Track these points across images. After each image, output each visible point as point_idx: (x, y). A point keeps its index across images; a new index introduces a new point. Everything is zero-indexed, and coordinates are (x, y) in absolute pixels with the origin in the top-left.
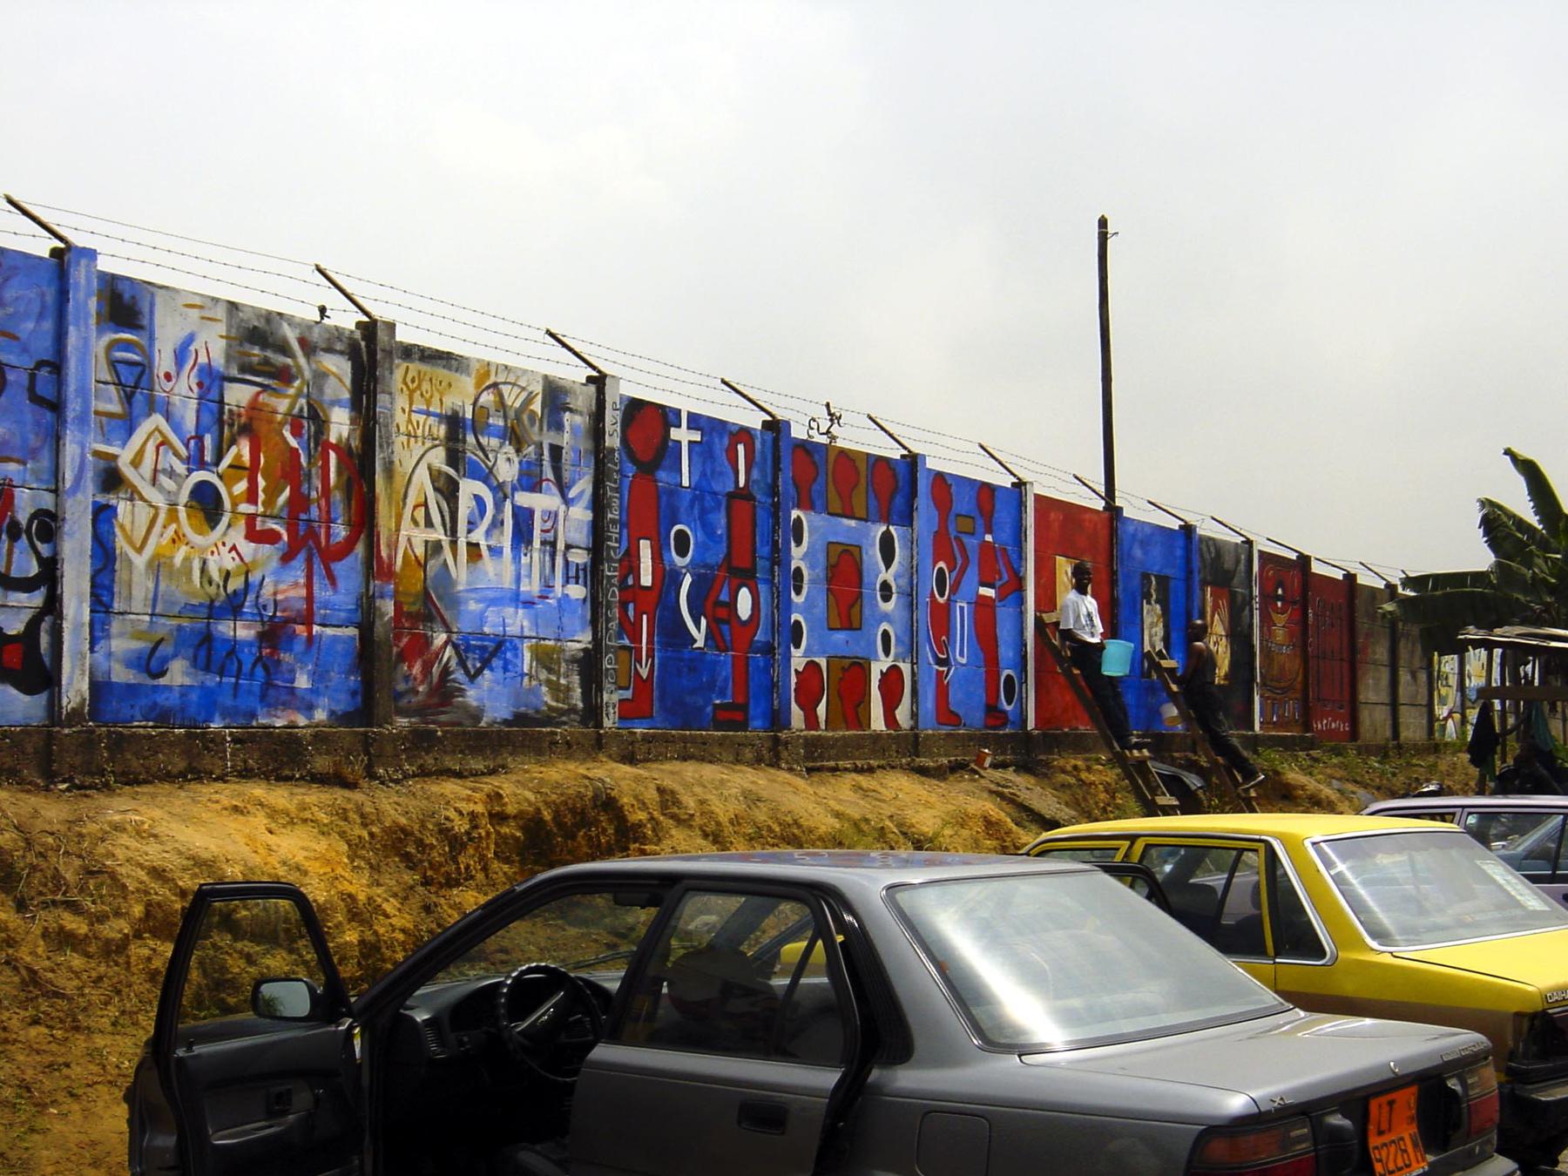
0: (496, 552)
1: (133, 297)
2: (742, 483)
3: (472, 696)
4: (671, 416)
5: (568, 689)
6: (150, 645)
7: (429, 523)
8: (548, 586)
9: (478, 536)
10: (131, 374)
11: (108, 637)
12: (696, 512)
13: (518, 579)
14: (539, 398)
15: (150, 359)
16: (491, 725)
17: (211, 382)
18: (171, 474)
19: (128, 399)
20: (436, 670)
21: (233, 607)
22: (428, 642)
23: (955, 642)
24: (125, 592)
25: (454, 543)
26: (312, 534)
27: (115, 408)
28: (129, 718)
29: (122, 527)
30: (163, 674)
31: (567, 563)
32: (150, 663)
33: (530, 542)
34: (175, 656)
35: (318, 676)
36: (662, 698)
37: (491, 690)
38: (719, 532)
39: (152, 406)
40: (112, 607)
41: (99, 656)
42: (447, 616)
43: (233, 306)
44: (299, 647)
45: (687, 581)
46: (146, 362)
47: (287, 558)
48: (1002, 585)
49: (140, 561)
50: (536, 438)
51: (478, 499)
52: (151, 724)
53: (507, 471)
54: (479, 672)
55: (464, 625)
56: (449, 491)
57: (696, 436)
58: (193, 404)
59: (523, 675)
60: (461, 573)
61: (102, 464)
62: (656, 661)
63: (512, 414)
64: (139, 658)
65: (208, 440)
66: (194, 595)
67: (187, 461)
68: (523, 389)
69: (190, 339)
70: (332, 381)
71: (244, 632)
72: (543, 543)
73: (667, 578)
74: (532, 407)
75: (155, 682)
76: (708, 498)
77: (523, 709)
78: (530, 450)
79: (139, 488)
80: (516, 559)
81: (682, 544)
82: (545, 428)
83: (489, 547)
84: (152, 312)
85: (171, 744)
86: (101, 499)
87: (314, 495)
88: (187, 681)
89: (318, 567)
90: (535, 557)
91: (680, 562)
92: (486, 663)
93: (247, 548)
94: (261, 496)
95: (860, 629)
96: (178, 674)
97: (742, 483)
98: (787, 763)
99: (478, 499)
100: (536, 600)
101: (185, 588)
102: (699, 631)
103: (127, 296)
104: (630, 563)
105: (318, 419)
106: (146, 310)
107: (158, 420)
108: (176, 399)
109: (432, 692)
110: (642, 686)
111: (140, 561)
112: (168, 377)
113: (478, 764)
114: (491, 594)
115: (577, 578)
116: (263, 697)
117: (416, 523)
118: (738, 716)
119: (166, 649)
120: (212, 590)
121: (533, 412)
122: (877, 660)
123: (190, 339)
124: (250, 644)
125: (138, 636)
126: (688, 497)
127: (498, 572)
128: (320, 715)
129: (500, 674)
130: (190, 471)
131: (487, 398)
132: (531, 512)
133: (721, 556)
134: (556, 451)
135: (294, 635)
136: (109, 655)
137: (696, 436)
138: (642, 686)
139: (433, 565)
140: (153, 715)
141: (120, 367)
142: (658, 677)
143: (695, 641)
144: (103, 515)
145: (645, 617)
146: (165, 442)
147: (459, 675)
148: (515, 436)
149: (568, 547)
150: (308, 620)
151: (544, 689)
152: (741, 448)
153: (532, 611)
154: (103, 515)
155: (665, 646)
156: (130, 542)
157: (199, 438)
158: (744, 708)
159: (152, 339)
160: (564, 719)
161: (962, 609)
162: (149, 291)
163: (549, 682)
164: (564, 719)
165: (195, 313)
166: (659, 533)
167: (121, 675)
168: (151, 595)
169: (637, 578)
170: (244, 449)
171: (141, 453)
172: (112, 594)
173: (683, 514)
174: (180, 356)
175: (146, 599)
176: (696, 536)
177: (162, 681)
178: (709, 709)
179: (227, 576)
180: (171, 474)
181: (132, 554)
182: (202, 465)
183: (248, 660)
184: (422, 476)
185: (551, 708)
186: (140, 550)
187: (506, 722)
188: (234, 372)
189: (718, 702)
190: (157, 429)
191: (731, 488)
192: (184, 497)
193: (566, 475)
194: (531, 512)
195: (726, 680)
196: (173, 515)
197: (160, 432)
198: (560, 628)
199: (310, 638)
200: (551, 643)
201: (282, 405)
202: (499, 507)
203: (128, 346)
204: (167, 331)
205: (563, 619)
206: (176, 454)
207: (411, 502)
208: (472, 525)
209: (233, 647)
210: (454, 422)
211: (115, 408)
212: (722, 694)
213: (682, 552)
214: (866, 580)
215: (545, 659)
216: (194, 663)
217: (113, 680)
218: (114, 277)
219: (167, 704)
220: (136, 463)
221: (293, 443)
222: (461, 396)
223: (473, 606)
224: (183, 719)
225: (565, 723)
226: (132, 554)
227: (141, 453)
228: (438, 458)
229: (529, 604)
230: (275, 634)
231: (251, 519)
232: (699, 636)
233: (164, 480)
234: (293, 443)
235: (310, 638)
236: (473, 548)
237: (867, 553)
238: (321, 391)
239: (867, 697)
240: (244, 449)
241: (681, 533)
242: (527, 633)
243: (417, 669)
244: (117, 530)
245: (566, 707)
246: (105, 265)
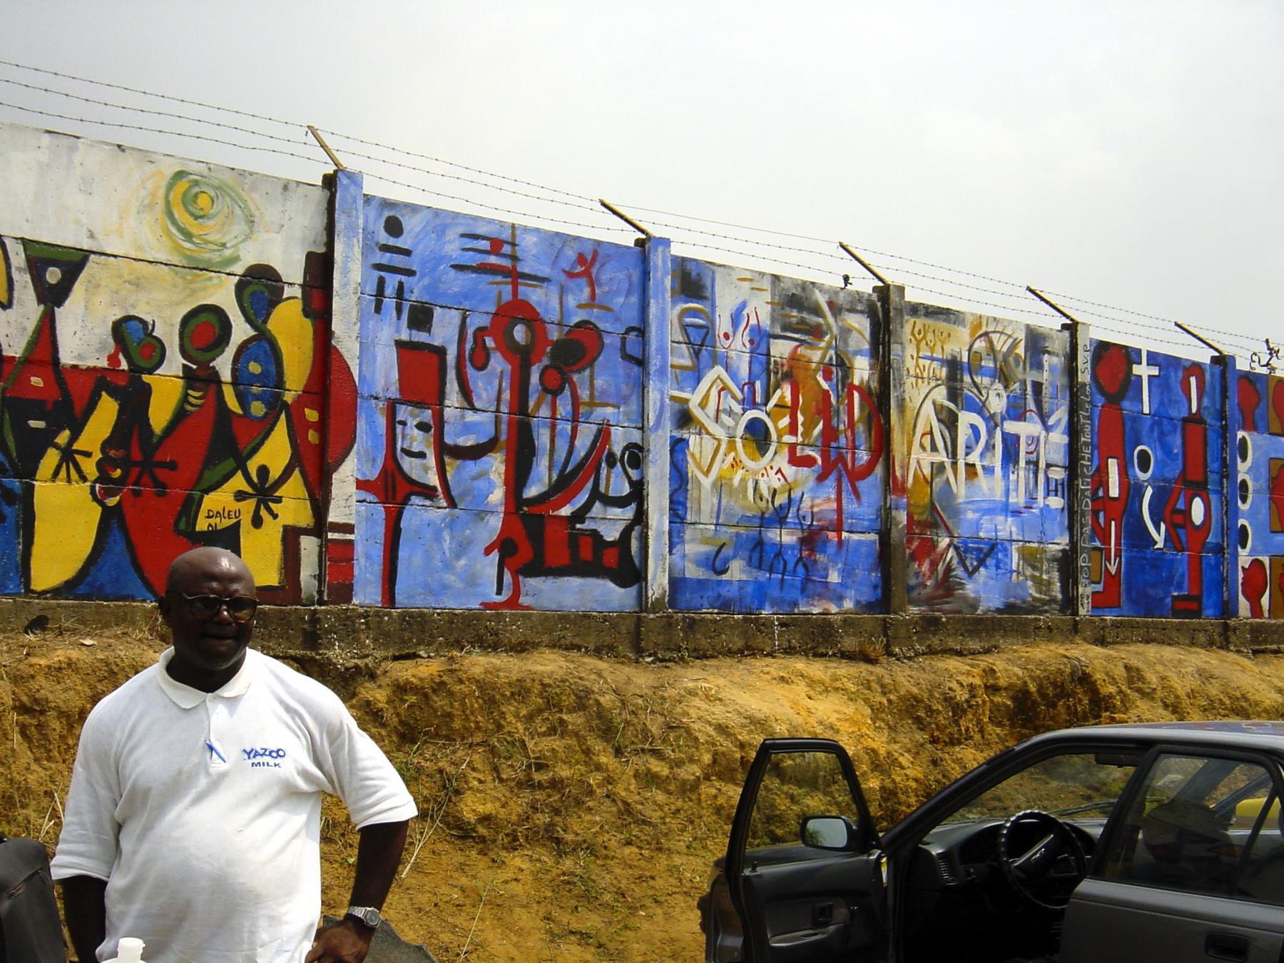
0: (989, 470)
1: (698, 275)
2: (1194, 410)
3: (970, 589)
4: (1134, 356)
5: (1049, 583)
6: (716, 549)
7: (934, 448)
8: (1032, 498)
9: (974, 458)
10: (699, 335)
11: (683, 542)
12: (1156, 434)
14: (1022, 344)
15: (713, 322)
16: (985, 613)
17: (760, 339)
18: (730, 413)
19: (697, 354)
20: (941, 568)
21: (779, 518)
22: (934, 545)
24: (695, 507)
25: (954, 464)
26: (841, 459)
27: (687, 362)
28: (699, 605)
29: (693, 455)
30: (725, 571)
31: (1047, 479)
32: (716, 564)
33: (1017, 462)
34: (734, 557)
35: (846, 573)
36: (1129, 591)
37: (985, 584)
38: (1176, 451)
39: (715, 360)
40: (685, 518)
41: (676, 557)
42: (949, 523)
43: (776, 278)
44: (831, 550)
45: (1149, 492)
46: (709, 325)
47: (821, 478)
49: (707, 482)
50: (1020, 376)
51: (974, 428)
52: (716, 611)
53: (997, 404)
54: (976, 569)
55: (963, 531)
56: (950, 422)
57: (1155, 371)
58: (746, 357)
59: (1012, 572)
60: (960, 488)
61: (677, 406)
62: (1123, 560)
63: (1000, 357)
64: (707, 559)
65: (758, 385)
66: (749, 509)
67: (742, 402)
68: (1010, 336)
69: (743, 305)
70: (855, 334)
71: (788, 537)
72: (1028, 463)
73: (1131, 490)
74: (1017, 351)
75: (719, 578)
76: (1165, 422)
77: (1012, 600)
79: (706, 425)
80: (1006, 476)
81: (1144, 463)
82: (1028, 369)
83: (983, 467)
84: (713, 286)
85: (732, 627)
86: (677, 434)
87: (842, 427)
88: (744, 577)
89: (846, 485)
90: (1021, 473)
91: (1143, 476)
92: (982, 562)
93: (790, 471)
94: (801, 429)
96: (737, 571)
97: (1194, 410)
99: (974, 428)
100: (1023, 510)
101: (741, 502)
102: (1159, 533)
103: (694, 274)
104: (1101, 479)
105: (844, 366)
106: (708, 284)
107: (719, 370)
108: (733, 354)
109: (938, 585)
110: (1111, 580)
111: (707, 482)
112: (726, 336)
113: (974, 645)
114: (985, 506)
115: (1056, 491)
116: (803, 590)
117: (923, 447)
118: (1194, 606)
119: (727, 551)
120: (763, 504)
121: (1018, 356)
123: (743, 305)
124: (792, 547)
125: (705, 541)
126: (1149, 422)
127: (991, 487)
128: (848, 605)
129: (993, 570)
130: (745, 411)
131: (980, 345)
132: (1017, 438)
133: (1178, 471)
134: (1037, 387)
135: (827, 540)
136: (684, 556)
137: (1155, 371)
138: (1111, 580)
139: (938, 482)
140: (719, 603)
141: (690, 330)
142: (1126, 573)
143: (1156, 543)
144: (678, 446)
145: (1113, 523)
147: (959, 572)
148: (1003, 376)
149: (1048, 466)
150: (839, 529)
151: (1030, 583)
152: (1193, 380)
153: (1019, 519)
154: (678, 446)
155: (1130, 546)
156: (699, 466)
157: (751, 384)
158: (1198, 599)
159: (713, 306)
160: (1046, 608)
162: (710, 269)
163: (1033, 578)
164: (1046, 608)
165: (746, 285)
167: (693, 572)
168: (716, 509)
169: (1107, 490)
170: (786, 391)
171: (706, 397)
172: (686, 508)
173: (1145, 439)
174: (735, 320)
175: (712, 512)
176: (1156, 458)
177: (725, 577)
178: (1168, 600)
180: (730, 413)
181: (701, 477)
182: (754, 405)
183: (791, 558)
184: (929, 409)
185: (1035, 599)
186: (707, 473)
187: (998, 610)
188: (778, 331)
189: (1176, 594)
190: (718, 377)
191: (1185, 414)
192: (740, 431)
193: (1046, 407)
194: (1017, 438)
195: (1182, 576)
196: (732, 445)
197: (721, 380)
199: (840, 542)
200: (1035, 545)
202: (991, 434)
203: (695, 313)
204: (725, 300)
205: (1045, 525)
206: (734, 397)
207: (919, 431)
208: (969, 449)
209: (780, 550)
210: (953, 366)
211: (687, 362)
212: (1179, 587)
213: (1144, 468)
215: (1030, 558)
216: (750, 563)
217: (687, 576)
218: (684, 259)
219: (730, 595)
220: (703, 405)
221: (825, 385)
222: (959, 344)
223: (970, 515)
224: (741, 607)
225: (1046, 611)
226: (701, 477)
227: (706, 397)
228: (941, 394)
229: (1016, 513)
231: (792, 447)
232: (1159, 538)
233: (724, 417)
234: (825, 385)
235: (840, 543)
236: (970, 467)
238: (846, 343)
240: (786, 391)
241: (1142, 453)
242: (1015, 537)
243: (925, 567)
244: (689, 459)
245: (1047, 598)
246: (677, 250)
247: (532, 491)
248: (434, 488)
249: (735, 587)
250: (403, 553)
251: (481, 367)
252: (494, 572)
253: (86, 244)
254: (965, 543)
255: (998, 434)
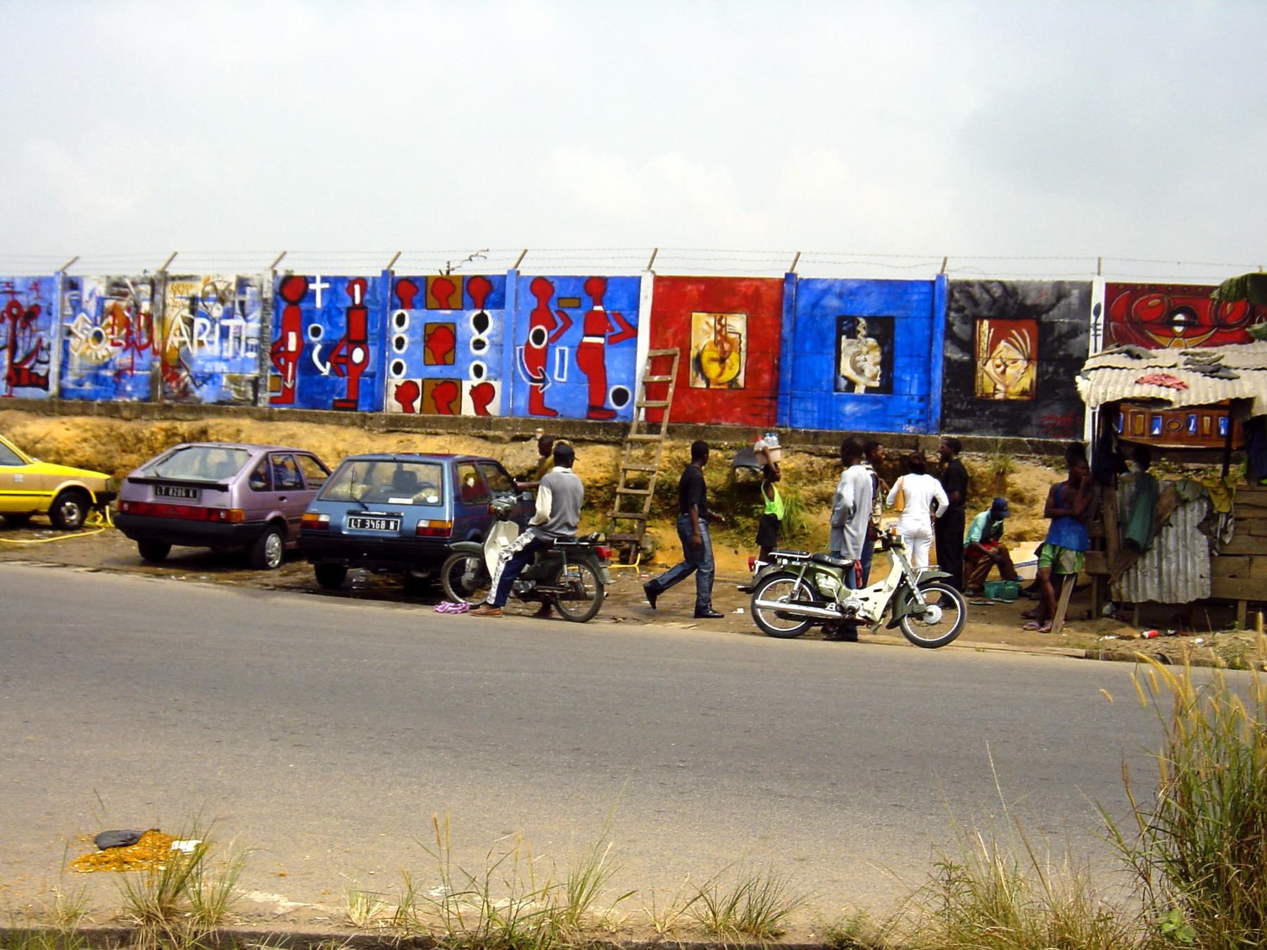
0: (211, 343)
2: (357, 301)
3: (198, 394)
5: (245, 392)
7: (181, 335)
9: (203, 338)
13: (222, 351)
16: (206, 404)
17: (101, 301)
18: (87, 329)
20: (182, 385)
21: (106, 366)
22: (178, 375)
23: (554, 368)
25: (192, 342)
26: (134, 342)
31: (247, 344)
32: (79, 383)
35: (135, 387)
39: (82, 310)
42: (188, 366)
43: (108, 277)
44: (128, 378)
47: (125, 350)
48: (613, 336)
51: (204, 326)
54: (201, 385)
55: (195, 369)
56: (190, 323)
59: (222, 386)
60: (194, 351)
62: (297, 381)
65: (99, 319)
70: (143, 293)
71: (109, 373)
72: (235, 338)
73: (304, 348)
78: (229, 305)
81: (316, 332)
89: (136, 352)
91: (313, 339)
93: (111, 348)
94: (116, 332)
95: (453, 364)
97: (357, 301)
98: (369, 426)
104: (284, 340)
105: (137, 306)
109: (181, 392)
113: (189, 417)
117: (175, 335)
118: (352, 405)
122: (468, 378)
127: (213, 350)
128: (135, 399)
134: (242, 304)
135: (126, 374)
146: (85, 321)
147: (192, 386)
148: (221, 300)
149: (247, 338)
150: (132, 369)
151: (233, 392)
157: (96, 318)
158: (356, 402)
161: (562, 353)
163: (235, 389)
166: (300, 329)
170: (110, 319)
173: (316, 318)
174: (91, 295)
177: (82, 388)
179: (104, 357)
180: (87, 329)
183: (110, 381)
184: (179, 321)
187: (214, 404)
188: (108, 297)
189: (337, 398)
191: (349, 304)
193: (247, 311)
194: (228, 328)
195: (343, 389)
196: (87, 341)
198: (243, 369)
201: (124, 304)
202: (213, 327)
204: (87, 287)
207: (173, 329)
208: (200, 334)
209: (105, 378)
210: (194, 300)
212: (339, 394)
214: (459, 338)
215: (234, 381)
216: (93, 383)
221: (127, 314)
222: (197, 289)
223: (200, 362)
228: (186, 313)
229: (227, 360)
230: (120, 374)
231: (112, 340)
232: (325, 370)
235: (133, 375)
237: (461, 326)
239: (459, 397)
240: (110, 319)
243: (174, 384)
255: (217, 326)
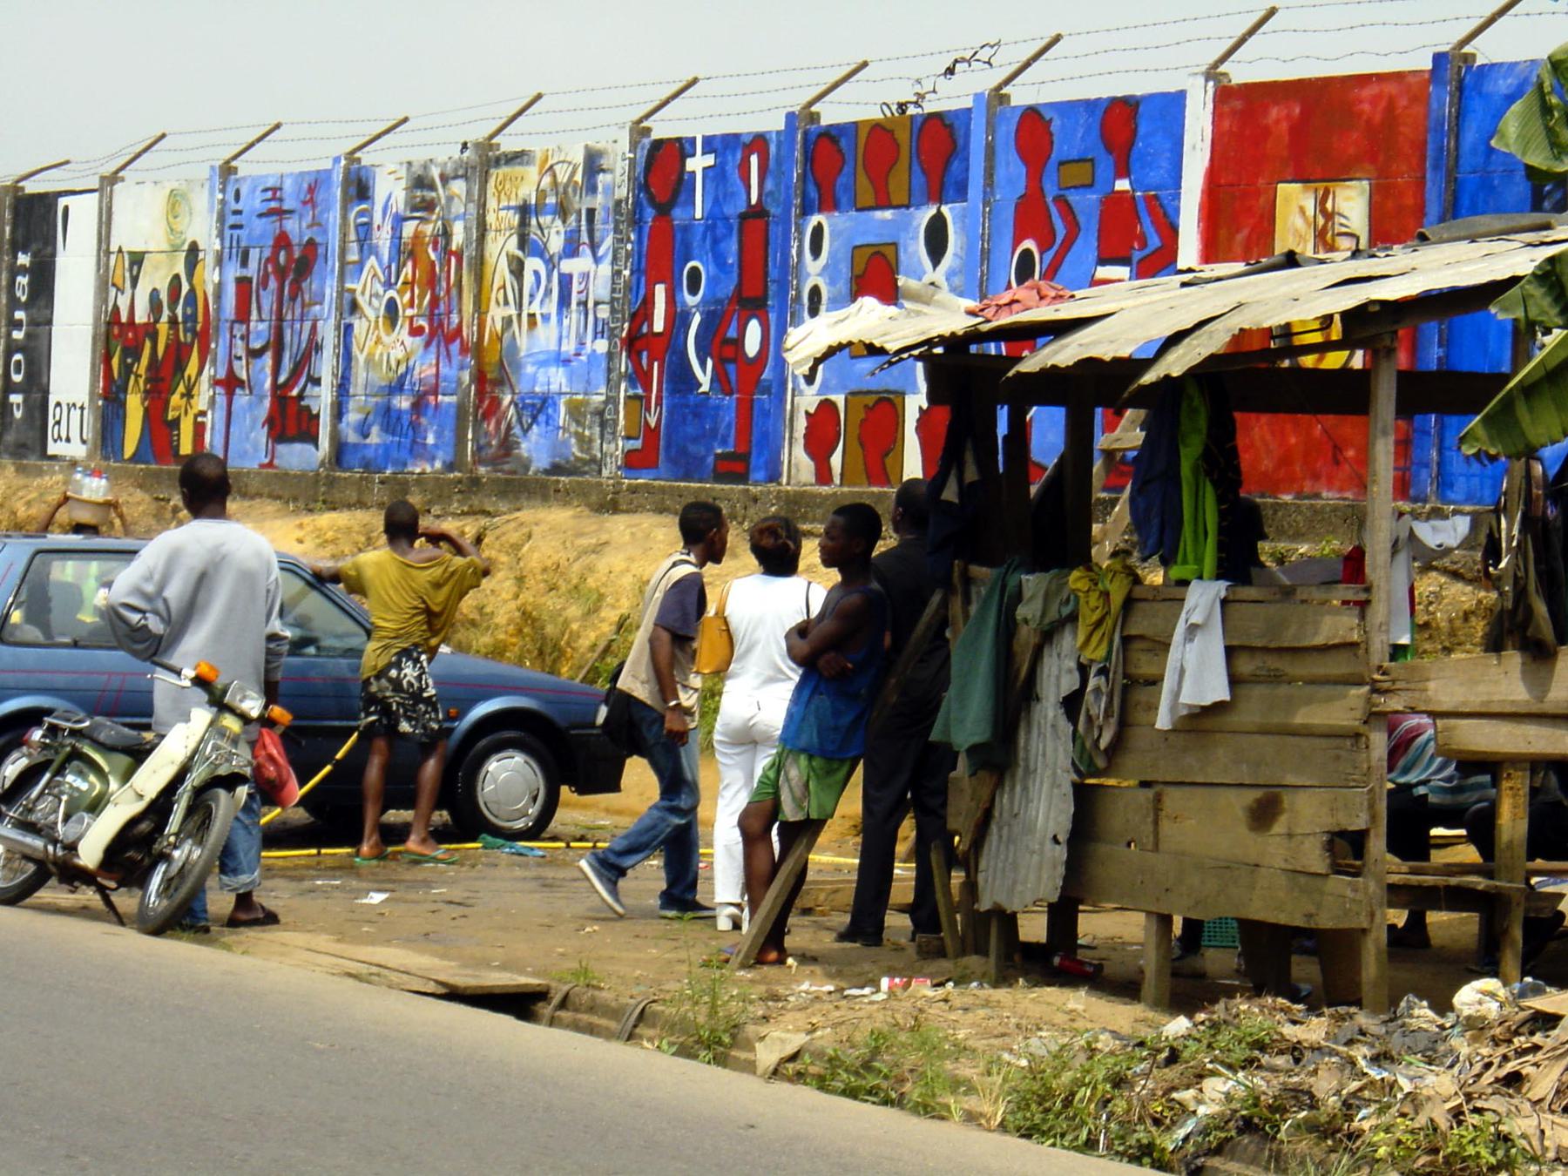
2: (754, 201)
4: (687, 146)
5: (591, 440)
7: (506, 303)
8: (582, 344)
9: (535, 308)
12: (708, 242)
14: (580, 170)
17: (399, 220)
20: (503, 426)
25: (519, 315)
31: (596, 319)
33: (569, 305)
36: (668, 446)
37: (537, 443)
38: (730, 261)
44: (430, 412)
45: (697, 320)
47: (428, 345)
50: (576, 206)
51: (536, 273)
53: (556, 244)
54: (530, 426)
55: (522, 387)
56: (517, 270)
57: (710, 160)
59: (559, 428)
60: (523, 342)
63: (561, 190)
68: (570, 163)
72: (579, 304)
73: (678, 319)
76: (719, 224)
77: (557, 459)
80: (560, 322)
83: (542, 315)
87: (442, 294)
90: (574, 316)
91: (691, 301)
92: (534, 419)
93: (409, 340)
94: (416, 301)
96: (375, 437)
97: (754, 201)
99: (536, 273)
100: (572, 358)
102: (704, 372)
110: (651, 434)
114: (542, 357)
115: (603, 332)
116: (411, 451)
118: (738, 467)
119: (371, 418)
120: (391, 374)
121: (576, 183)
124: (406, 412)
126: (701, 229)
128: (438, 465)
131: (547, 180)
132: (570, 276)
133: (732, 288)
134: (591, 213)
137: (710, 160)
138: (651, 434)
139: (507, 336)
142: (668, 426)
143: (700, 385)
145: (656, 364)
147: (517, 430)
149: (596, 304)
151: (573, 441)
152: (754, 159)
155: (673, 392)
157: (389, 267)
160: (586, 468)
164: (586, 468)
169: (651, 325)
173: (696, 252)
176: (708, 272)
178: (710, 460)
181: (358, 353)
185: (577, 459)
186: (362, 351)
188: (408, 214)
189: (719, 451)
191: (742, 208)
193: (597, 235)
194: (570, 276)
196: (377, 327)
199: (437, 405)
200: (580, 397)
205: (592, 374)
207: (495, 288)
212: (724, 442)
213: (694, 290)
215: (576, 412)
220: (363, 293)
223: (530, 369)
225: (586, 473)
229: (567, 362)
232: (704, 379)
234: (433, 256)
236: (532, 316)
238: (450, 212)
241: (695, 270)
242: (564, 389)
243: (492, 427)
245: (588, 457)
247: (282, 379)
248: (243, 382)
249: (372, 450)
250: (232, 430)
251: (265, 289)
252: (264, 440)
253: (143, 249)
254: (523, 399)
